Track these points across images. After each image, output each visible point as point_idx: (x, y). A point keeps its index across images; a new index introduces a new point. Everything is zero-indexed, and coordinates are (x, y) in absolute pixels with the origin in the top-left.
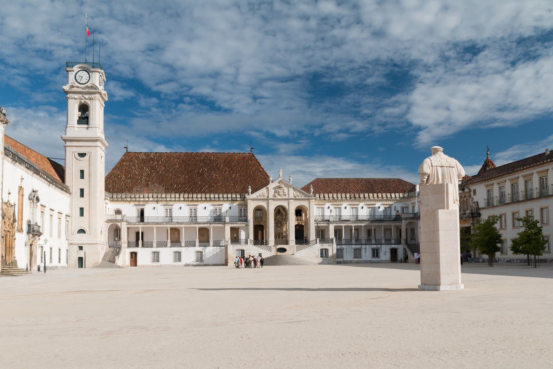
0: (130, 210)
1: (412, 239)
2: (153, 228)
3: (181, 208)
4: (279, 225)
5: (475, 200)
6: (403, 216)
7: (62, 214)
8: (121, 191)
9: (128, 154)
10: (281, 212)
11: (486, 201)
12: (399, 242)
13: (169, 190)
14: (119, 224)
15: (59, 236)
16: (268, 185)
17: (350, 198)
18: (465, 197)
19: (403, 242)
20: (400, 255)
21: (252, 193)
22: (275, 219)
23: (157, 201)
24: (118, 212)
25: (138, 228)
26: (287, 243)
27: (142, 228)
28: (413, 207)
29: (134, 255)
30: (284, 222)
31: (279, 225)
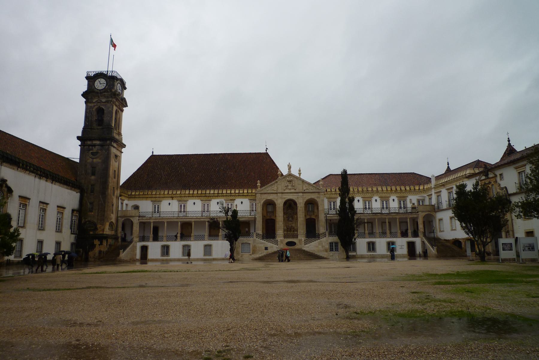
0: (146, 206)
1: (431, 232)
2: (164, 223)
3: (194, 203)
4: (290, 219)
5: (502, 186)
6: (420, 208)
7: (64, 208)
8: (141, 188)
9: (153, 155)
10: (290, 205)
11: (518, 185)
12: (415, 234)
13: (185, 187)
14: (131, 219)
15: (59, 230)
16: (276, 179)
17: (363, 191)
18: (490, 183)
19: (421, 234)
20: (419, 249)
21: (261, 187)
22: (284, 213)
23: (172, 198)
24: (136, 207)
25: (150, 223)
26: (296, 236)
27: (154, 222)
28: (430, 199)
29: (144, 249)
30: (296, 216)
31: (290, 219)
